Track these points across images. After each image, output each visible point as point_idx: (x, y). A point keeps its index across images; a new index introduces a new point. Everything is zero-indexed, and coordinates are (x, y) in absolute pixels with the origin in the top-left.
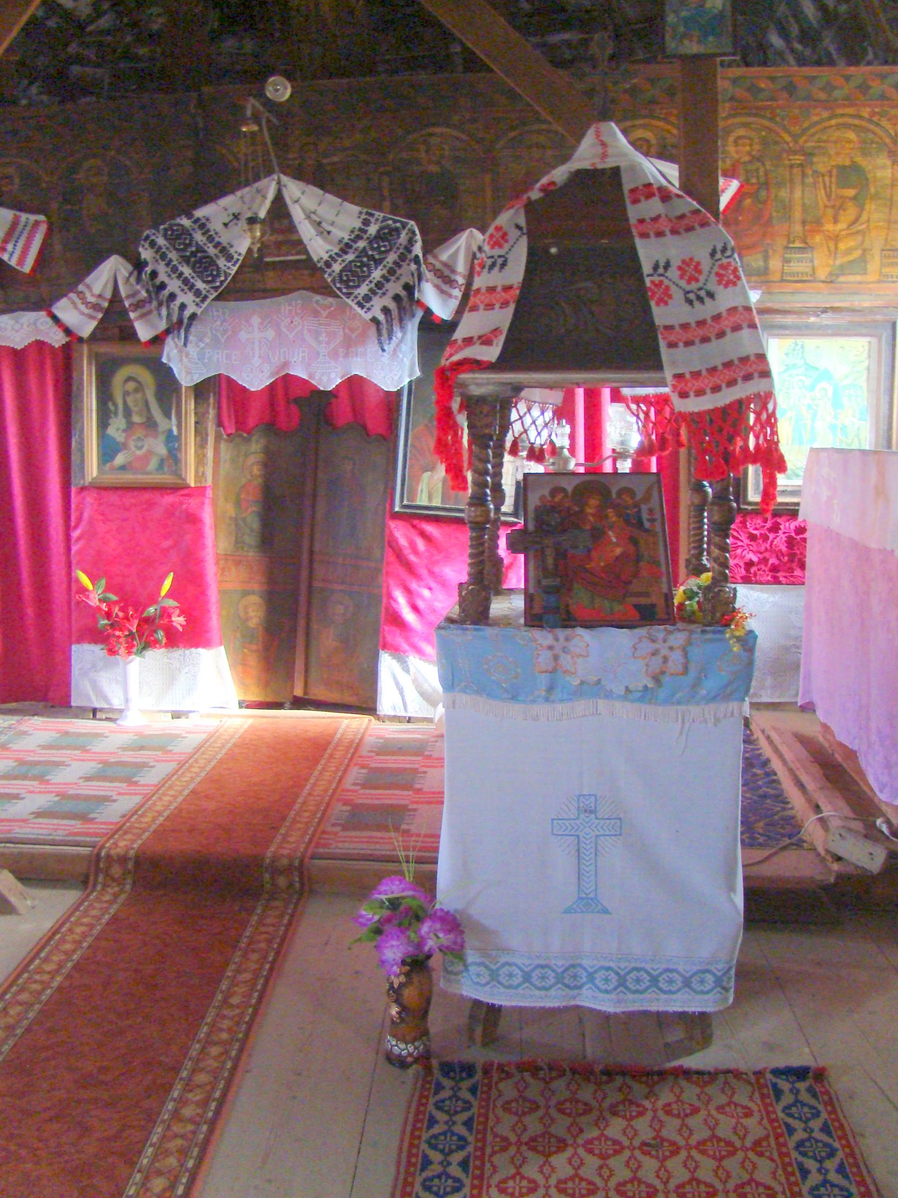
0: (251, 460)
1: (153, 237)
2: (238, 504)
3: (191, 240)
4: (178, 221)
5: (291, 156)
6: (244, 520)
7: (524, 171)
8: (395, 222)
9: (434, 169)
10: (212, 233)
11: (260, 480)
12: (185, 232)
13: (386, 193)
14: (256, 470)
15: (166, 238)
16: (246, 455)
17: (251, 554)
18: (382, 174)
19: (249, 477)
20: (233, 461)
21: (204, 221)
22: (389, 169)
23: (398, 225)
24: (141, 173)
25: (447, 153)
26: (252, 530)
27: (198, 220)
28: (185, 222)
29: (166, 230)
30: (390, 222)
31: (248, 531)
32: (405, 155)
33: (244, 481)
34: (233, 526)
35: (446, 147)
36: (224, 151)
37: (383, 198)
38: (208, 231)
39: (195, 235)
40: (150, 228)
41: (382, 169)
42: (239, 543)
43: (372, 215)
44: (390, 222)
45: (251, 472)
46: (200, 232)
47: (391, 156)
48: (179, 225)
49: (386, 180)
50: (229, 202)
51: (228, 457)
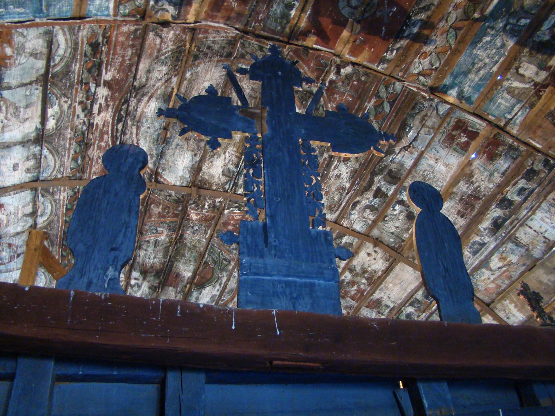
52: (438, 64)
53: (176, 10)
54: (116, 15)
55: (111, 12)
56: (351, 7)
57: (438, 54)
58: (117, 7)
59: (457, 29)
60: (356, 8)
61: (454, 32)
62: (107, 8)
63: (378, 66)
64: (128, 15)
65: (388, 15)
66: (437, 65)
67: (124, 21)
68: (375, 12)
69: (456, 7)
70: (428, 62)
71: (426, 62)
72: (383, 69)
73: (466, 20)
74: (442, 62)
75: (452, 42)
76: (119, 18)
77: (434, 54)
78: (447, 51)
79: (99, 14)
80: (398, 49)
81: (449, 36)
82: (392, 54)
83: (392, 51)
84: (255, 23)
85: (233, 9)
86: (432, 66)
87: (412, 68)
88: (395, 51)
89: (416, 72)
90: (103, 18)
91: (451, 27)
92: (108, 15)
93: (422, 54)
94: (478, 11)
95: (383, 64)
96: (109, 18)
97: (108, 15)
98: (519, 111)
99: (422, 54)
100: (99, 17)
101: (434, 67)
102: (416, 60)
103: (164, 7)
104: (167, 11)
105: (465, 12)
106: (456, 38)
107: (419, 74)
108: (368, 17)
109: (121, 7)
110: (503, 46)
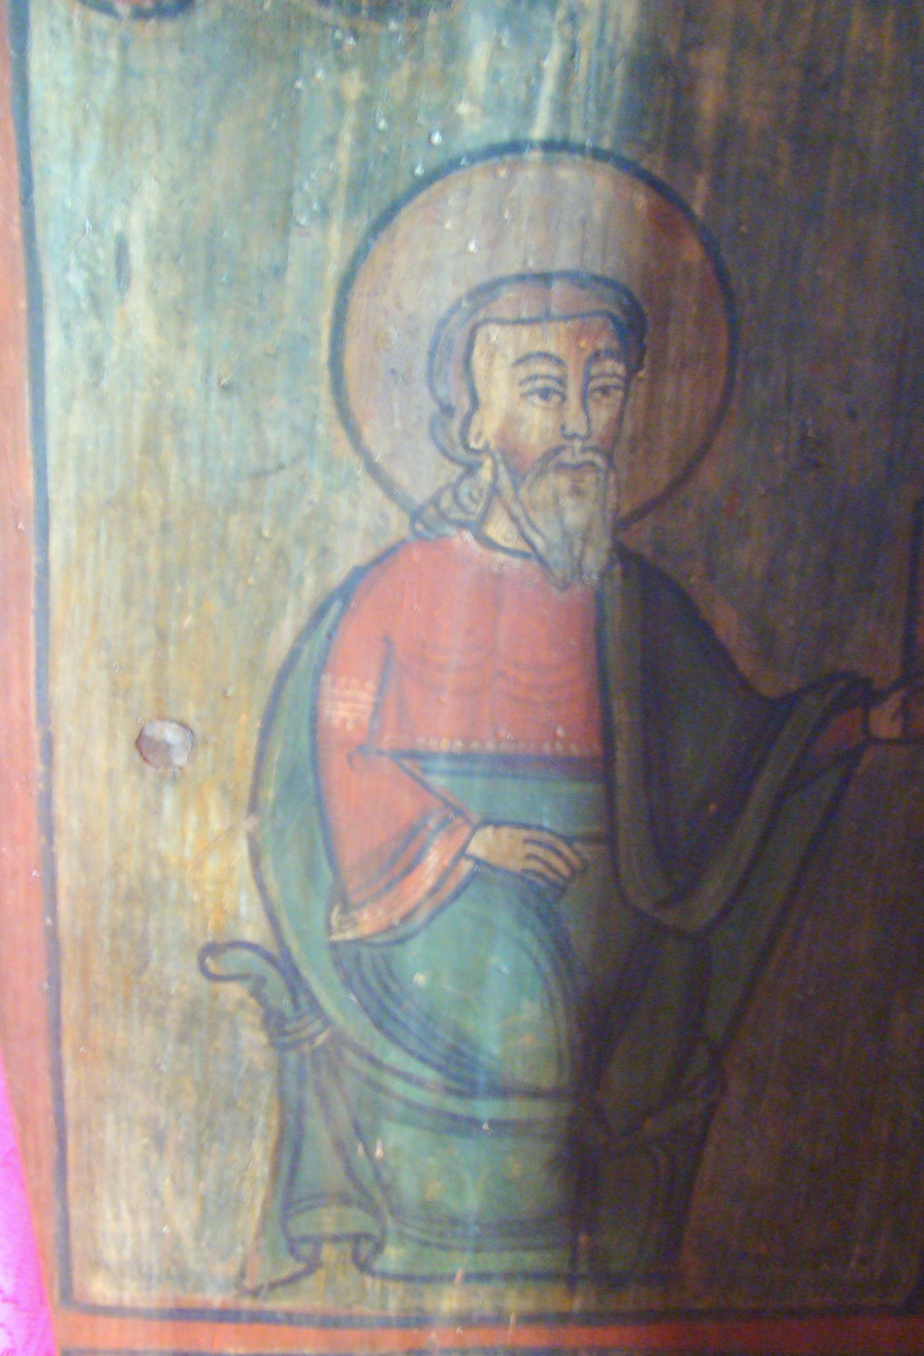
0: (450, 249)
2: (294, 786)
6: (373, 978)
11: (566, 520)
14: (528, 390)
16: (385, 205)
17: (449, 1301)
19: (424, 474)
20: (210, 271)
26: (460, 1067)
31: (414, 1081)
33: (360, 523)
34: (253, 1039)
42: (316, 1199)
45: (452, 419)
51: (139, 217)
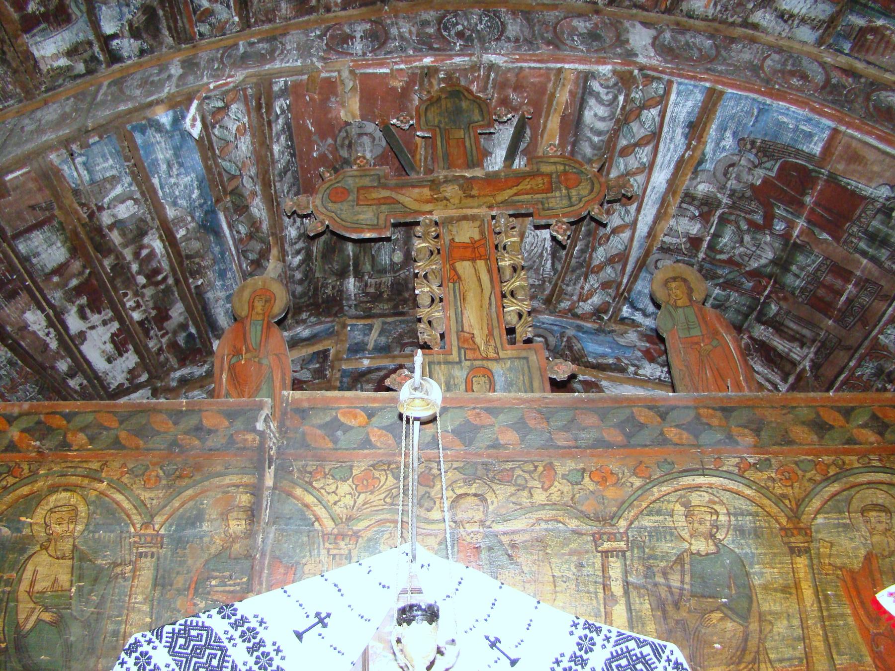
1: (145, 648)
3: (223, 660)
4: (203, 617)
5: (435, 515)
7: (863, 552)
8: (641, 644)
9: (701, 546)
10: (269, 648)
12: (213, 643)
13: (617, 588)
15: (171, 648)
18: (606, 554)
21: (254, 624)
22: (623, 545)
23: (647, 650)
24: (146, 525)
25: (723, 518)
27: (244, 620)
28: (218, 624)
29: (175, 635)
30: (632, 645)
32: (647, 522)
35: (722, 510)
36: (309, 499)
37: (610, 598)
38: (261, 643)
39: (231, 651)
40: (141, 628)
41: (606, 546)
43: (598, 630)
44: (632, 645)
46: (242, 646)
47: (622, 524)
48: (203, 627)
49: (616, 569)
50: (310, 592)
52: (216, 133)
53: (590, 86)
54: (670, 83)
55: (675, 86)
56: (366, 134)
57: (228, 143)
58: (667, 92)
59: (234, 177)
60: (360, 135)
61: (233, 173)
62: (679, 94)
63: (286, 82)
64: (654, 78)
65: (318, 145)
66: (216, 132)
67: (661, 72)
68: (336, 141)
69: (254, 194)
70: (230, 127)
71: (233, 127)
72: (276, 82)
73: (233, 190)
74: (214, 138)
75: (225, 164)
76: (666, 77)
77: (233, 139)
78: (221, 152)
79: (691, 88)
80: (278, 117)
81: (234, 167)
82: (280, 107)
83: (283, 112)
84: (479, 75)
85: (515, 90)
86: (220, 127)
87: (242, 107)
88: (279, 112)
89: (234, 107)
90: (686, 81)
91: (241, 175)
92: (680, 84)
93: (245, 130)
94: (230, 205)
95: (281, 89)
96: (679, 80)
97: (680, 84)
98: (79, 175)
99: (245, 130)
100: (692, 83)
101: (217, 126)
102: (246, 120)
103: (606, 91)
104: (601, 85)
105: (241, 195)
106: (225, 170)
107: (227, 107)
108: (340, 131)
109: (661, 92)
110: (175, 204)
